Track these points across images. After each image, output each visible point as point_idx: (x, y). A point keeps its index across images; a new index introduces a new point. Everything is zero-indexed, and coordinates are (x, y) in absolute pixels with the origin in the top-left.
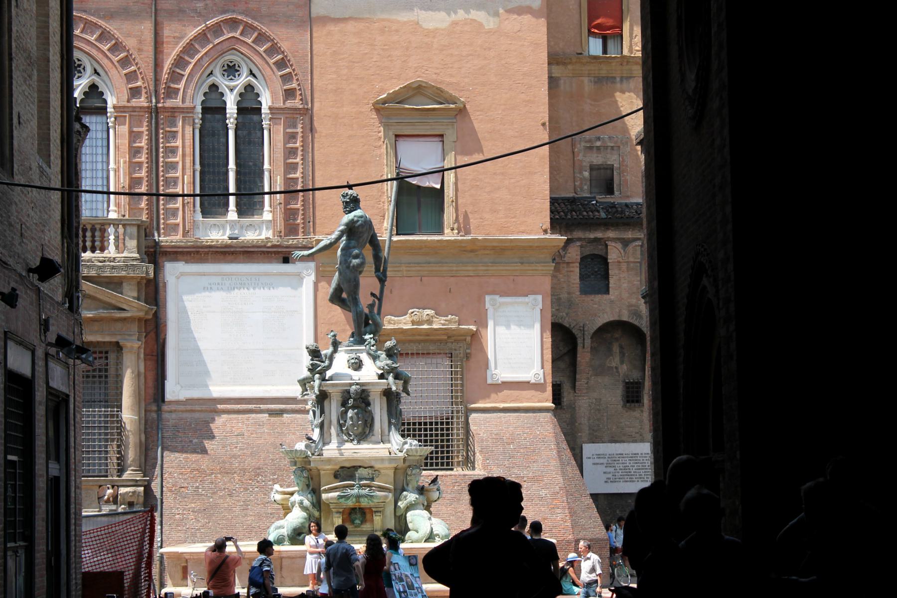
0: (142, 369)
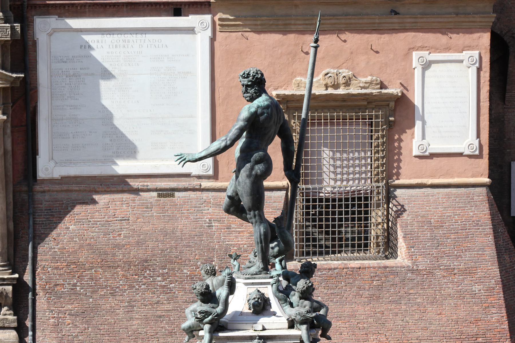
0: (9, 147)
